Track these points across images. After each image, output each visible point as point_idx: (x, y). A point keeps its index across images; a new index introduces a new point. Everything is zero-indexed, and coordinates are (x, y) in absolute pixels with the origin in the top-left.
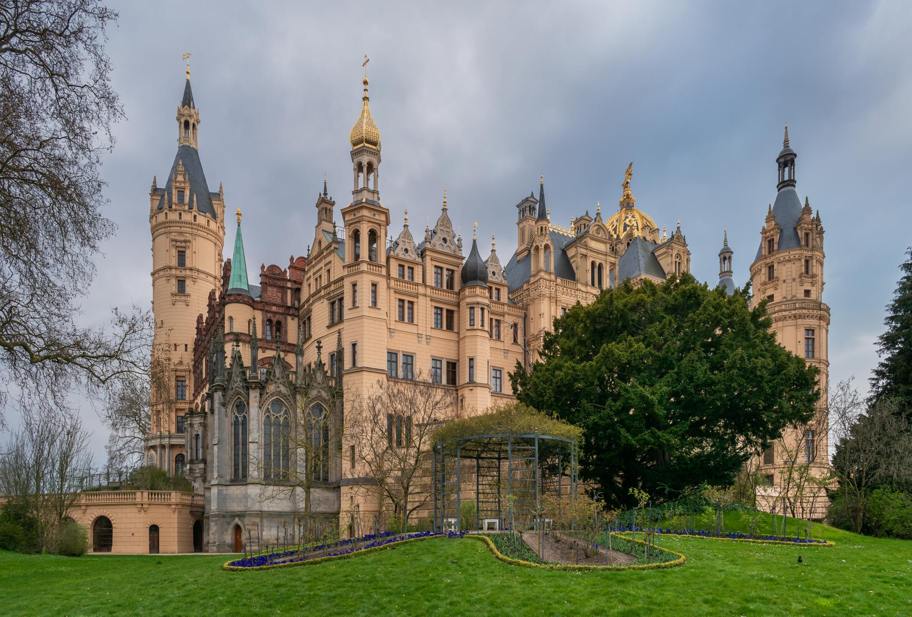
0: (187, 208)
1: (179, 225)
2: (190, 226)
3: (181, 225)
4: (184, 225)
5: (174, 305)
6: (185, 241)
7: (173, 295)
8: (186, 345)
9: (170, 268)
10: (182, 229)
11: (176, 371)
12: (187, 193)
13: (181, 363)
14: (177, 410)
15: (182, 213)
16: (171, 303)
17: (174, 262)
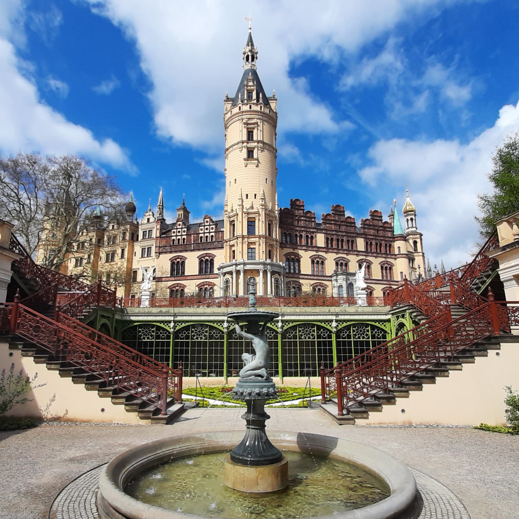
0: (255, 101)
1: (250, 113)
2: (257, 114)
3: (251, 113)
4: (253, 113)
5: (246, 166)
6: (254, 124)
7: (245, 160)
8: (255, 195)
9: (243, 142)
10: (252, 116)
11: (248, 213)
12: (254, 93)
13: (252, 208)
14: (249, 243)
15: (252, 105)
16: (244, 166)
17: (245, 138)
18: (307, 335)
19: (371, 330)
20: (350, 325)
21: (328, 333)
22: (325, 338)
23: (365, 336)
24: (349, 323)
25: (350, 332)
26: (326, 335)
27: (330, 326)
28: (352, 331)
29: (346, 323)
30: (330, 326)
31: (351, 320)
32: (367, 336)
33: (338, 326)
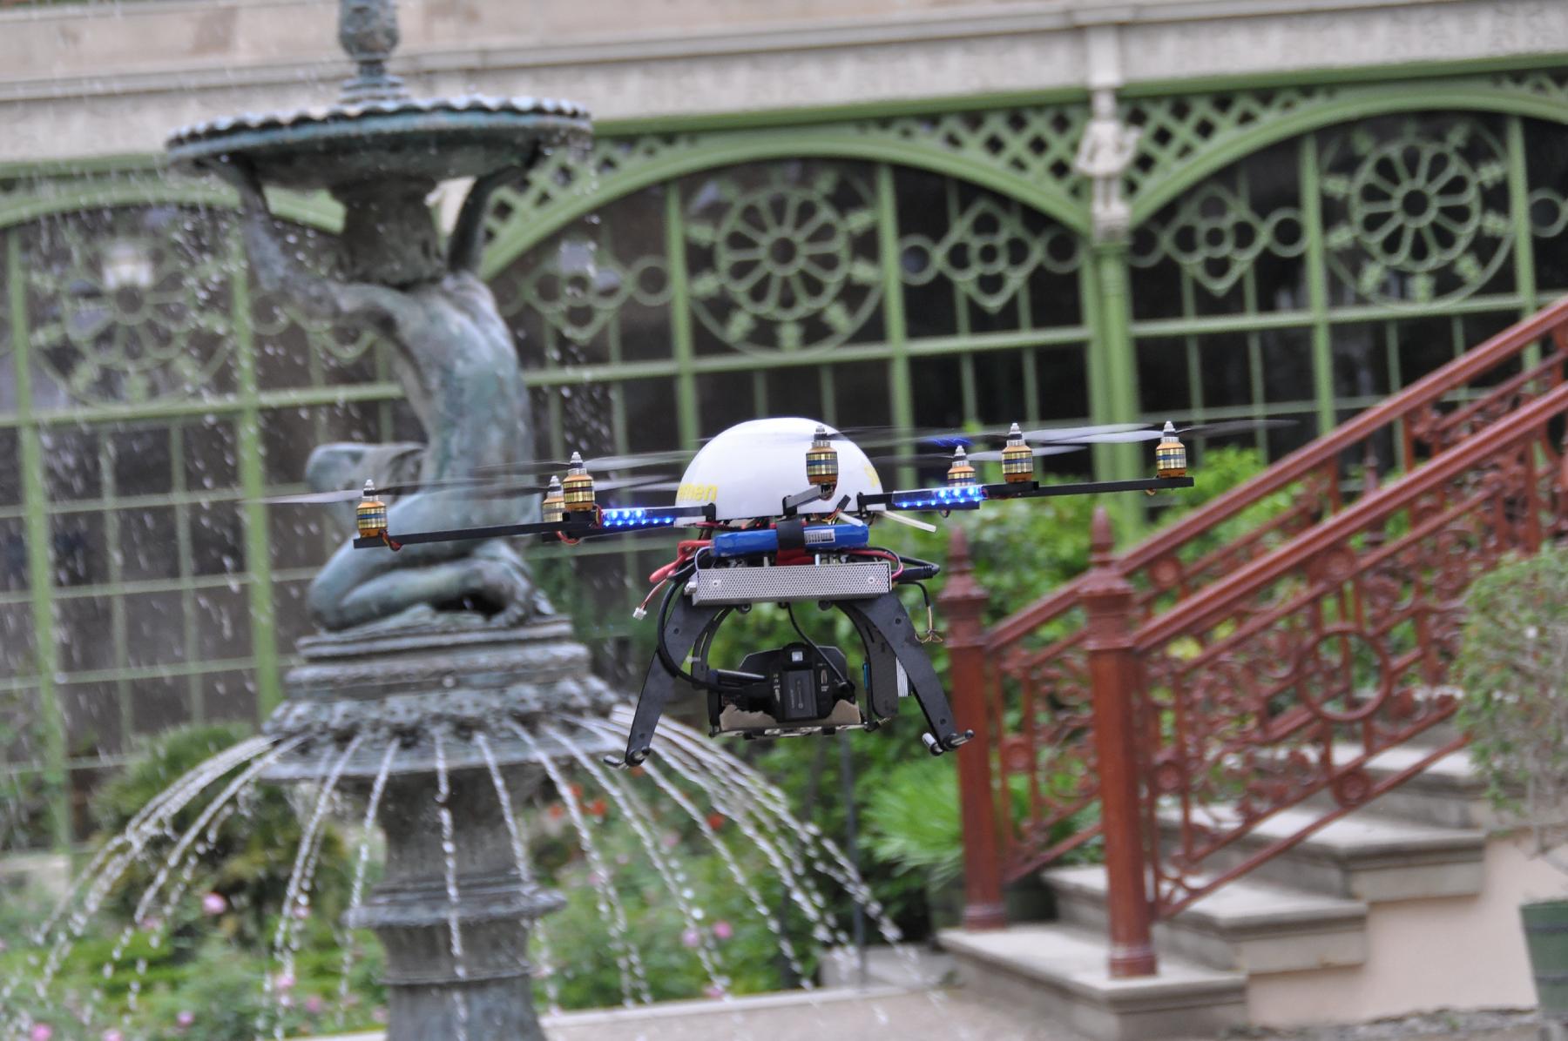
18: (787, 302)
19: (1533, 183)
20: (1287, 148)
21: (1038, 253)
22: (1007, 320)
23: (1468, 267)
24: (1273, 124)
25: (1290, 232)
26: (1016, 280)
27: (1060, 169)
28: (1311, 216)
29: (1246, 118)
30: (1060, 169)
31: (1308, 86)
32: (1484, 261)
33: (1145, 162)
